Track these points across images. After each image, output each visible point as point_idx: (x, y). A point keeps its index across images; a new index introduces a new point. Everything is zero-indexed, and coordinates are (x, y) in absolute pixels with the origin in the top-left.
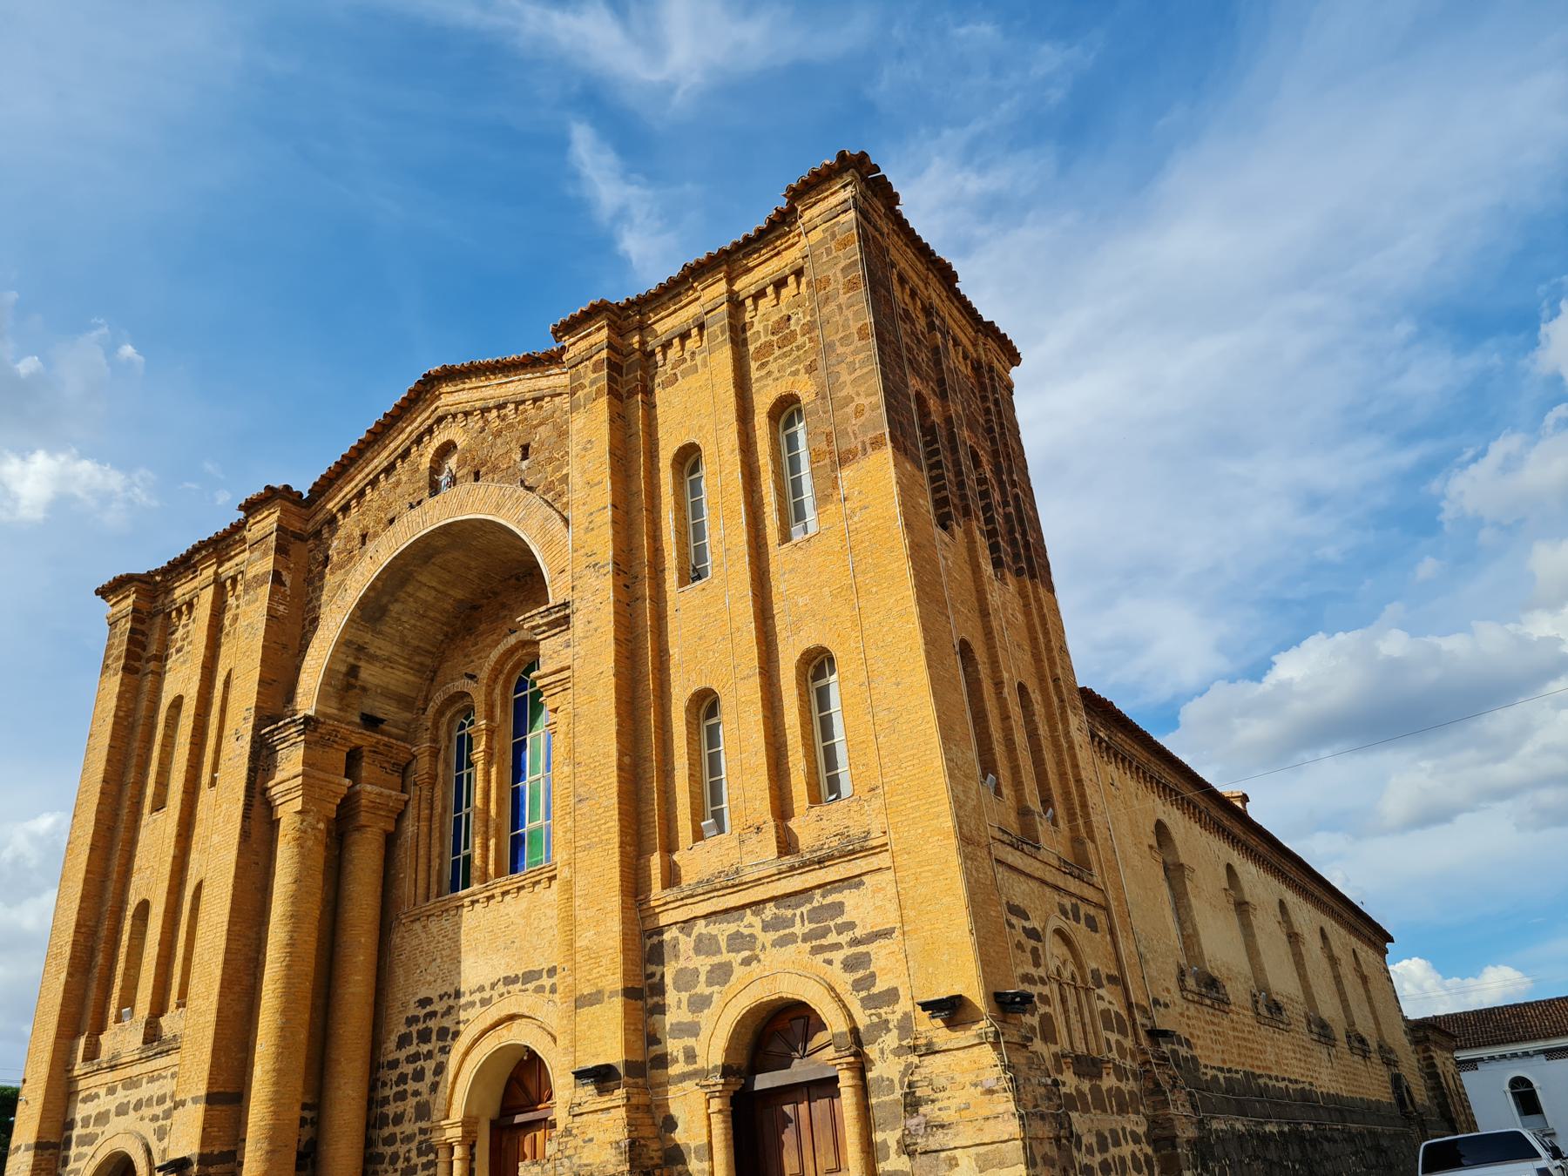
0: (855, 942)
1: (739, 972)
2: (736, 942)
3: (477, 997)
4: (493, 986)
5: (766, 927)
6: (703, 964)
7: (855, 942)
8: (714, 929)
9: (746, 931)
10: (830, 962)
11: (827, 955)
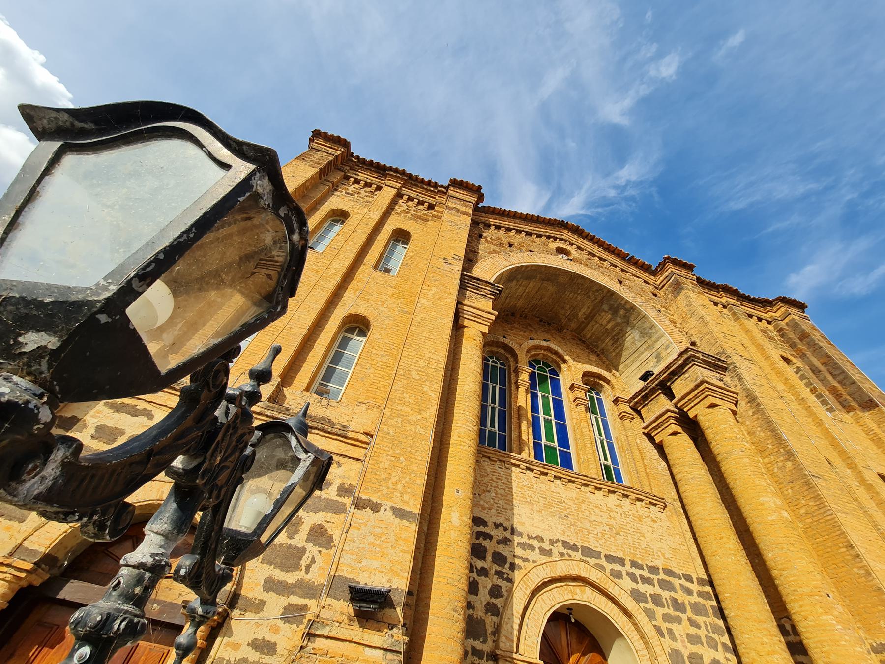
3: (536, 543)
4: (552, 542)
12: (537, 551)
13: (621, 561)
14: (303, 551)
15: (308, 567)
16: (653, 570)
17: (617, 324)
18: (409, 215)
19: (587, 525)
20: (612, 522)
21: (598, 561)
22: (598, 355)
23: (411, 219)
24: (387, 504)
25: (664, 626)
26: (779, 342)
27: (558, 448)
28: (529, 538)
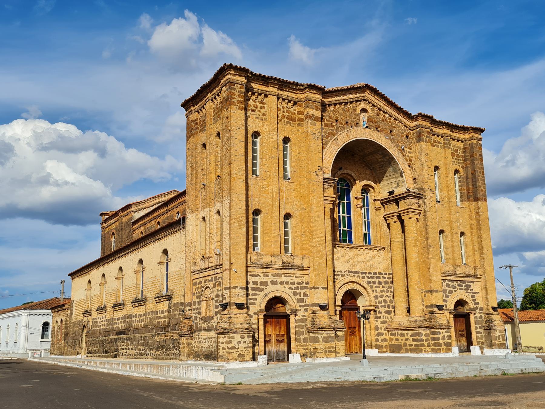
0: (473, 293)
1: (454, 292)
2: (453, 287)
3: (340, 273)
4: (345, 272)
5: (458, 285)
6: (448, 289)
7: (473, 293)
8: (449, 283)
9: (455, 285)
10: (469, 295)
11: (469, 294)
12: (340, 275)
13: (365, 273)
14: (303, 298)
15: (305, 302)
16: (375, 274)
17: (384, 161)
18: (285, 119)
19: (356, 263)
20: (365, 260)
21: (358, 275)
22: (371, 170)
24: (320, 287)
25: (374, 289)
26: (460, 158)
27: (347, 230)
28: (338, 272)
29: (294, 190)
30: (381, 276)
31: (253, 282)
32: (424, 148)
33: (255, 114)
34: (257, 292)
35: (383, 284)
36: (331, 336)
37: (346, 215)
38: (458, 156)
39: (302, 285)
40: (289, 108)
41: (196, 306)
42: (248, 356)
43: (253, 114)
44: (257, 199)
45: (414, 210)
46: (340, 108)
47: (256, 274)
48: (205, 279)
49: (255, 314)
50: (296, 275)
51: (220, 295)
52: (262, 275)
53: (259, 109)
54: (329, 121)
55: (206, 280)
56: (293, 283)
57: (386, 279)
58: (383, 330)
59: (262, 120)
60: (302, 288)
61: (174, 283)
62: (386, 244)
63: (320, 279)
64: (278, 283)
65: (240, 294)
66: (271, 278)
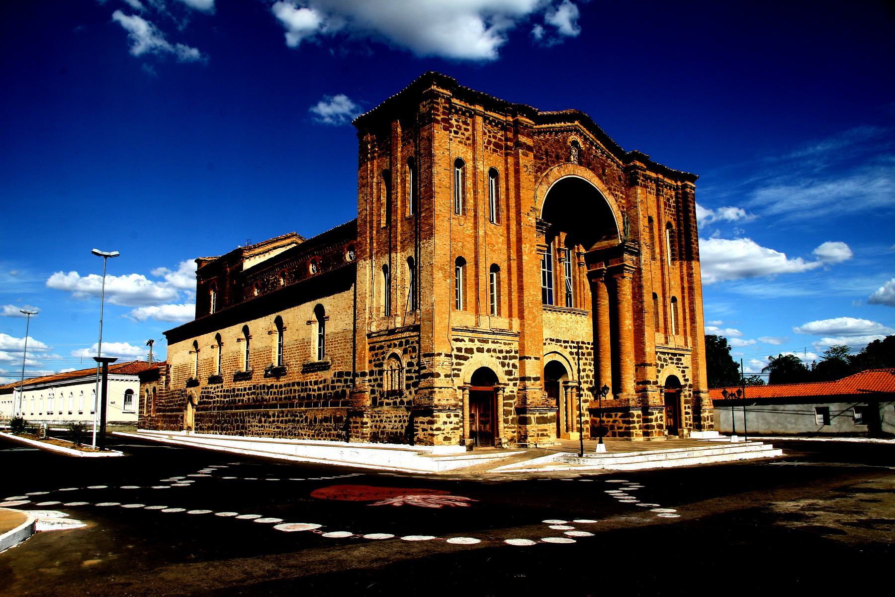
0: (683, 368)
2: (665, 360)
4: (546, 340)
7: (683, 368)
8: (661, 355)
13: (568, 342)
16: (578, 343)
19: (558, 330)
20: (567, 326)
23: (495, 151)
24: (532, 357)
29: (501, 235)
30: (584, 346)
31: (457, 348)
32: (640, 194)
33: (458, 137)
34: (462, 361)
35: (586, 356)
36: (543, 417)
37: (546, 270)
38: (670, 206)
39: (510, 354)
40: (496, 133)
41: (374, 377)
42: (454, 439)
43: (456, 137)
44: (460, 244)
45: (628, 268)
46: (550, 138)
47: (461, 338)
48: (389, 343)
49: (459, 388)
50: (505, 341)
51: (415, 363)
52: (466, 339)
53: (463, 131)
54: (539, 152)
55: (391, 344)
56: (501, 351)
57: (589, 350)
58: (585, 410)
59: (466, 145)
60: (511, 358)
61: (335, 347)
62: (589, 308)
63: (533, 347)
64: (485, 350)
65: (445, 363)
66: (478, 344)
